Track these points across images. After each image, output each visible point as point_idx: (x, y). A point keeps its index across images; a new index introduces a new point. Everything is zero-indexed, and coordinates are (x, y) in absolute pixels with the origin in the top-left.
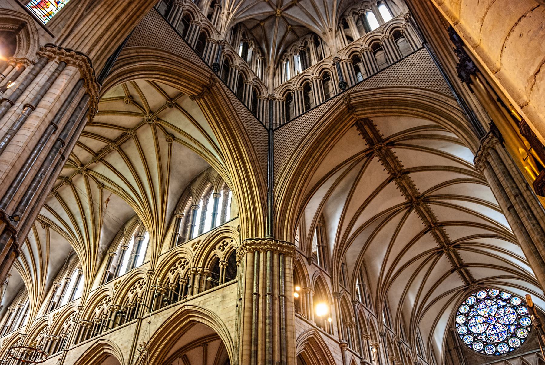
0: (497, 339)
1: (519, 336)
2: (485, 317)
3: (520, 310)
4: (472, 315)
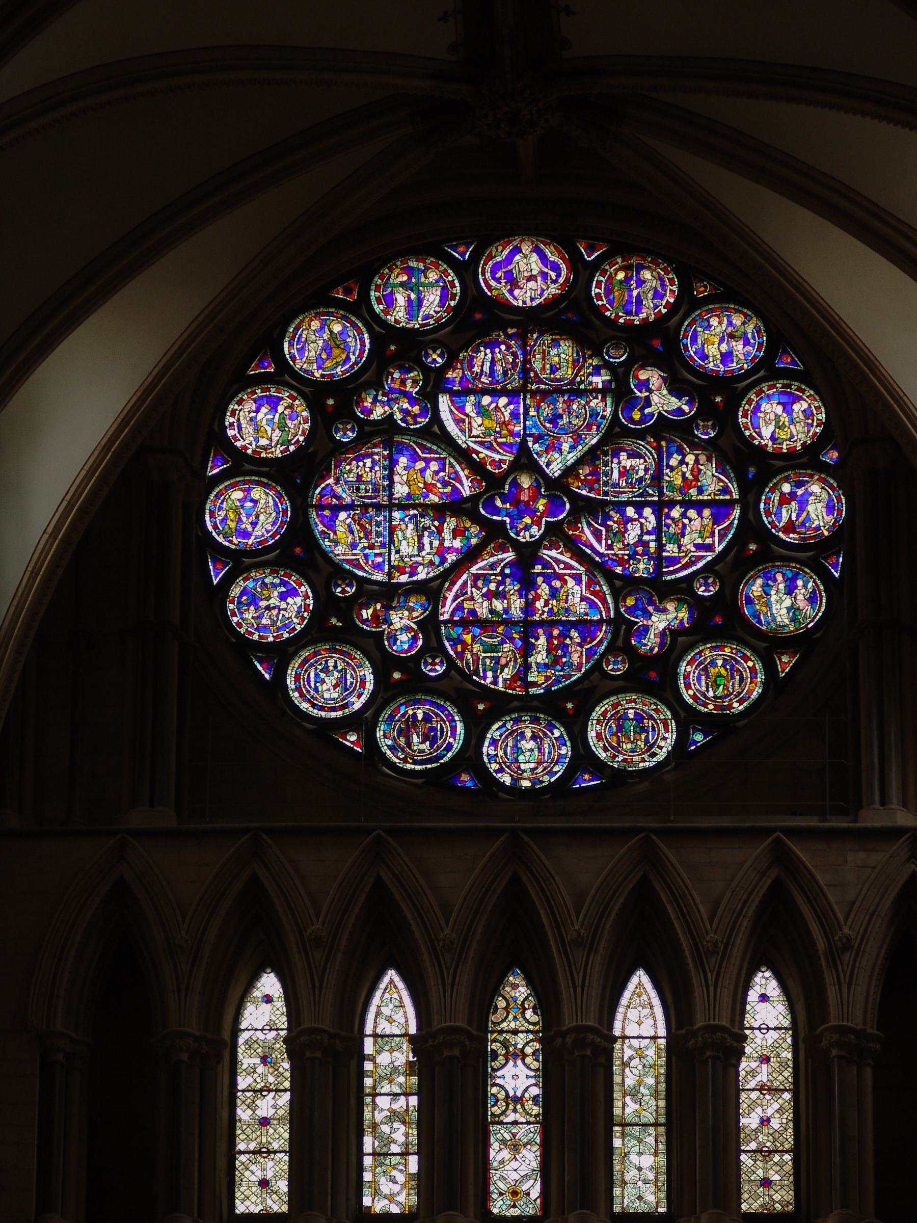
0: (507, 673)
1: (687, 696)
2: (477, 468)
3: (785, 500)
4: (378, 412)
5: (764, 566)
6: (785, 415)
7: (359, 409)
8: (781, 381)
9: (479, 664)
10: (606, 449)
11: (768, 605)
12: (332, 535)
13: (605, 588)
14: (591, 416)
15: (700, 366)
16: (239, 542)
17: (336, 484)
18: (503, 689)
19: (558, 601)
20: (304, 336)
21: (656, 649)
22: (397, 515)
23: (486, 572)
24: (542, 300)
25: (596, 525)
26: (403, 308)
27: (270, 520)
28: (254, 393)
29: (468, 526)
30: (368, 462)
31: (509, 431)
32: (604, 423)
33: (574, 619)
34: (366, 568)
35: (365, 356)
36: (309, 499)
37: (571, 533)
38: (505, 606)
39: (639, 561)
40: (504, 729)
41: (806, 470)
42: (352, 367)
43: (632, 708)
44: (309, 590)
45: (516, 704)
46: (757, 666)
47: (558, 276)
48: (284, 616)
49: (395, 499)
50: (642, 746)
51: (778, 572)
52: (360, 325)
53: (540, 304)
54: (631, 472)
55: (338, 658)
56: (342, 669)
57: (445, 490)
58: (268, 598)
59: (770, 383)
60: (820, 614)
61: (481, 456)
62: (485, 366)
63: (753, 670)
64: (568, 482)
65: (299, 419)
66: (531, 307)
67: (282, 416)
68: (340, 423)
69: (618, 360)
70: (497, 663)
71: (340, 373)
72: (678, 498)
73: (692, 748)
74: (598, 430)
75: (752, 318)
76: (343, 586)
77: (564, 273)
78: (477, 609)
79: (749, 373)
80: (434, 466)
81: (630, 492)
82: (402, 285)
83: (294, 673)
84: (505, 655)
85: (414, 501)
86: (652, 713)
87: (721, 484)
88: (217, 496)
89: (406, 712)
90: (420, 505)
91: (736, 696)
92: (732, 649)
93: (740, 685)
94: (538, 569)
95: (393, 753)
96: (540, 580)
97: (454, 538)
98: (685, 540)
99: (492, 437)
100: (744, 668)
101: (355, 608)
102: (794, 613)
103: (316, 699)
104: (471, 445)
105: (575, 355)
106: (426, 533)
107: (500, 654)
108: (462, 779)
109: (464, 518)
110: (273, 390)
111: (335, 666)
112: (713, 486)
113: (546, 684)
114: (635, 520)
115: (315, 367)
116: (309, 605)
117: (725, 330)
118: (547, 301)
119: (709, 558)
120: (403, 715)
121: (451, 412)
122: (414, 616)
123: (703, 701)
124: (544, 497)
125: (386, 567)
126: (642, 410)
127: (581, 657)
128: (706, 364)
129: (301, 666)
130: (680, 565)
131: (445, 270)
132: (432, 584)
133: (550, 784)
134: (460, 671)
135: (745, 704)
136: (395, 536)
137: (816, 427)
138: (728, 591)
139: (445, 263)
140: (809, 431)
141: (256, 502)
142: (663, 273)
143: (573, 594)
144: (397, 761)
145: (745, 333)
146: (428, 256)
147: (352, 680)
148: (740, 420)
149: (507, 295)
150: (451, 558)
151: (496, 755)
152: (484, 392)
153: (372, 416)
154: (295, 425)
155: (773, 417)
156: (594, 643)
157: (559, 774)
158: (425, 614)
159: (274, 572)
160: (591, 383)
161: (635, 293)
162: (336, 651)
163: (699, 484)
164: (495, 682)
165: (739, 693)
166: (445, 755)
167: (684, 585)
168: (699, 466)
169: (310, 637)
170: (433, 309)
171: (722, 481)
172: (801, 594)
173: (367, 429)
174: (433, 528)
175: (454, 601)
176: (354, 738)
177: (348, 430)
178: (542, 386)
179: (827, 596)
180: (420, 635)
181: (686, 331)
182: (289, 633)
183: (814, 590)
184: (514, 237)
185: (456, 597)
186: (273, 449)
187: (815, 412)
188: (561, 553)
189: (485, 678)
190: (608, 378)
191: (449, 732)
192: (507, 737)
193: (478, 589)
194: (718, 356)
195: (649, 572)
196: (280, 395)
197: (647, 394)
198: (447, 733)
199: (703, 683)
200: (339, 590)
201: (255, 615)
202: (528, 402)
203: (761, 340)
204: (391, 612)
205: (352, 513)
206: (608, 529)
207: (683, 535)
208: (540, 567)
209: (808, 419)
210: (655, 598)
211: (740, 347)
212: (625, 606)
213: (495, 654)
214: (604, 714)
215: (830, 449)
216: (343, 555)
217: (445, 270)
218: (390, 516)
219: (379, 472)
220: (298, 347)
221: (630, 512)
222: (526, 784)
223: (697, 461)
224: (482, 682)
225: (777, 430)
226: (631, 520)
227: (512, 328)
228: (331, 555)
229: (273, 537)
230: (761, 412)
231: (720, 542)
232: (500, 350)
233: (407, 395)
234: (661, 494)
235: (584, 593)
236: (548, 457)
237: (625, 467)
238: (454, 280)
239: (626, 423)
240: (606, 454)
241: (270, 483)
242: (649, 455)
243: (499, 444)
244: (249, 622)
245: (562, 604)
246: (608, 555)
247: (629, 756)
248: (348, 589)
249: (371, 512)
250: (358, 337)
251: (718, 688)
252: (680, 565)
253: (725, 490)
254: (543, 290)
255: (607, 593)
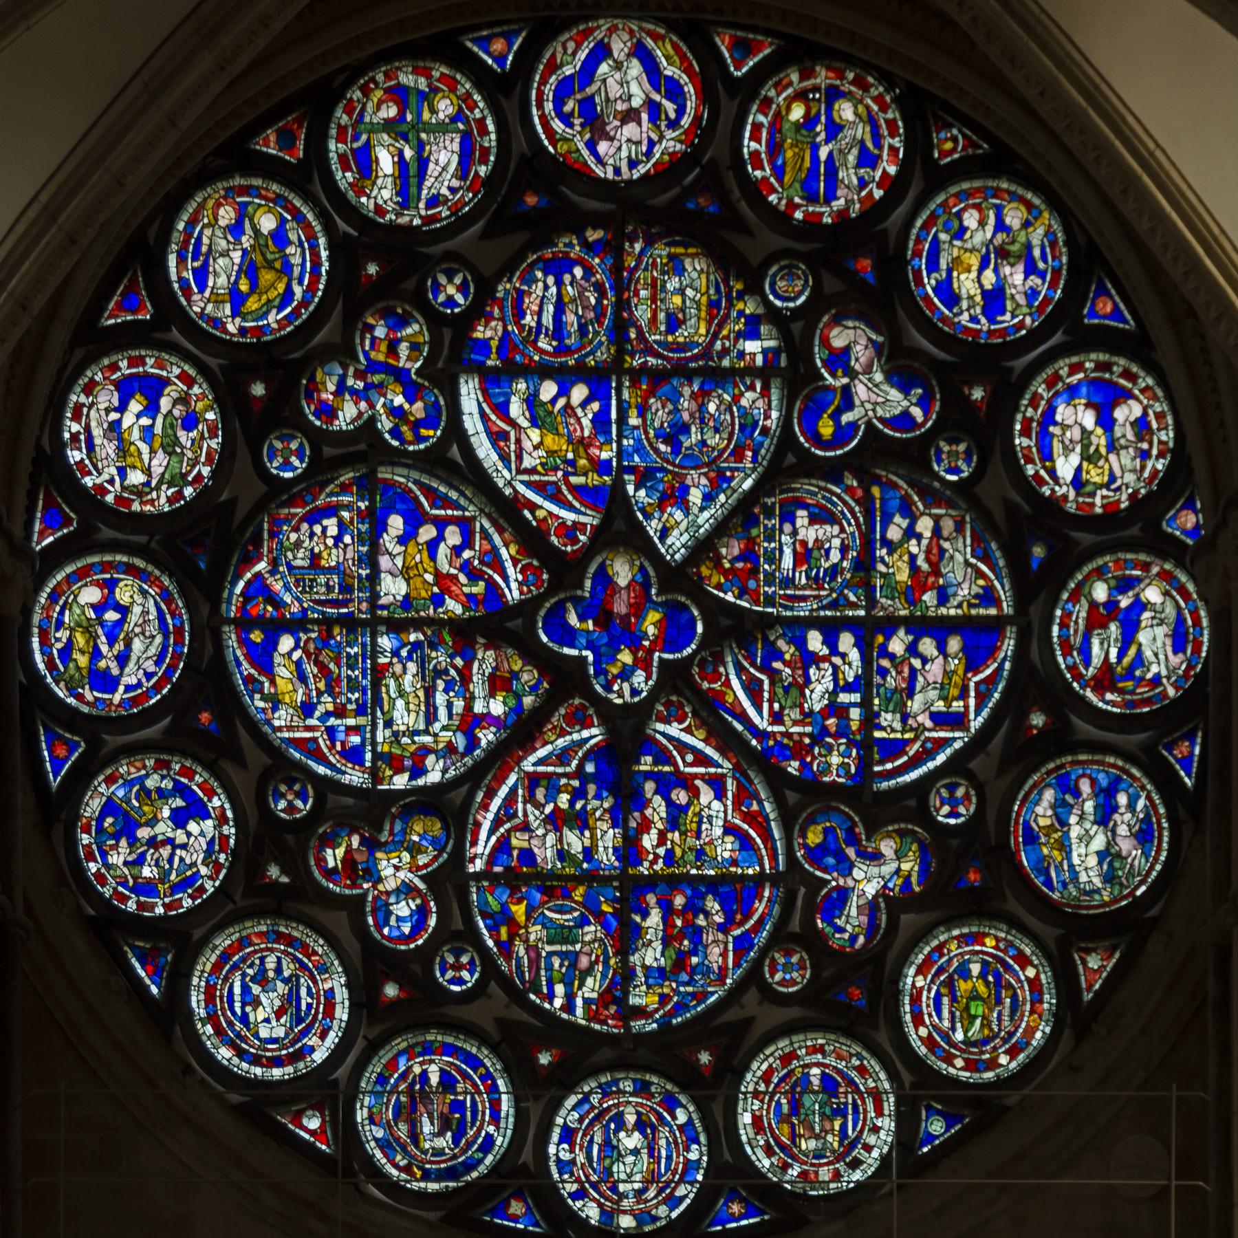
0: (591, 988)
1: (916, 1037)
3: (1099, 617)
4: (348, 412)
5: (1058, 762)
6: (1099, 431)
7: (313, 407)
8: (1093, 356)
9: (539, 969)
10: (769, 501)
11: (1064, 847)
12: (267, 685)
13: (768, 807)
14: (742, 428)
15: (944, 319)
16: (97, 699)
17: (273, 572)
18: (583, 1022)
19: (683, 834)
20: (205, 240)
21: (861, 940)
22: (385, 642)
23: (550, 769)
24: (649, 165)
25: (752, 670)
26: (390, 180)
27: (153, 651)
28: (114, 367)
29: (516, 668)
30: (332, 525)
31: (590, 459)
32: (766, 444)
33: (712, 872)
34: (331, 758)
35: (321, 287)
36: (224, 606)
37: (705, 685)
38: (587, 843)
39: (830, 749)
40: (586, 1107)
41: (1136, 552)
42: (296, 313)
43: (818, 1065)
44: (227, 806)
45: (606, 1054)
46: (1043, 977)
47: (681, 111)
48: (182, 860)
49: (383, 607)
50: (836, 1145)
51: (1084, 775)
52: (310, 217)
53: (645, 177)
54: (816, 554)
55: (283, 952)
56: (291, 976)
57: (475, 590)
58: (152, 822)
59: (1075, 359)
60: (1158, 867)
61: (541, 514)
62: (545, 314)
63: (1034, 984)
64: (699, 574)
65: (200, 427)
66: (630, 182)
67: (168, 421)
68: (277, 438)
69: (791, 305)
70: (574, 965)
71: (275, 326)
72: (903, 613)
73: (925, 1150)
74: (754, 460)
75: (1041, 213)
76: (290, 797)
77: (690, 105)
78: (536, 850)
79: (1036, 337)
80: (453, 536)
81: (815, 597)
82: (388, 125)
83: (203, 984)
84: (586, 949)
85: (417, 612)
86: (853, 1074)
87: (981, 582)
88: (54, 597)
89: (409, 1070)
90: (430, 621)
91: (1005, 1041)
92: (997, 939)
93: (1012, 1019)
94: (646, 763)
95: (386, 1155)
96: (650, 787)
97: (492, 694)
98: (915, 705)
99: (560, 474)
100: (1019, 981)
101: (312, 844)
102: (1110, 864)
103: (244, 1039)
104: (522, 489)
105: (712, 291)
106: (441, 685)
107: (578, 947)
108: (512, 1211)
109: (510, 651)
110: (150, 361)
111: (279, 970)
112: (965, 586)
113: (661, 1012)
114: (825, 659)
115: (228, 311)
116: (228, 837)
117: (991, 241)
118: (660, 168)
119: (958, 745)
120: (404, 1076)
121: (483, 415)
122: (421, 863)
123: (944, 1050)
124: (656, 606)
125: (368, 756)
126: (836, 416)
127: (724, 955)
128: (956, 315)
129: (217, 967)
130: (905, 758)
131: (468, 95)
132: (453, 794)
133: (671, 1223)
134: (506, 982)
135: (1021, 1057)
136: (384, 689)
137: (1157, 458)
138: (991, 817)
139: (469, 79)
140: (1143, 468)
141: (124, 610)
142: (875, 108)
143: (710, 817)
144: (395, 1172)
145: (1029, 247)
146: (434, 60)
147: (309, 1000)
148: (1017, 441)
149: (585, 153)
150: (487, 736)
151: (573, 1162)
152: (544, 372)
153: (337, 423)
154: (193, 441)
155: (1077, 436)
156: (747, 926)
157: (688, 1201)
158: (441, 860)
159: (161, 765)
160: (742, 354)
161: (823, 153)
162: (280, 937)
163: (941, 581)
164: (569, 1007)
165: (1011, 1034)
166: (480, 1161)
167: (912, 803)
168: (942, 542)
169: (231, 906)
170: (446, 183)
171: (982, 575)
172: (1124, 822)
173: (328, 451)
174: (453, 672)
175: (492, 832)
176: (314, 1123)
177: (292, 453)
178: (652, 361)
179: (1171, 829)
180: (432, 904)
181: (918, 241)
182: (192, 897)
183: (1148, 815)
184: (596, 18)
185: (497, 823)
186: (154, 495)
187: (1154, 425)
188: (687, 730)
189: (551, 996)
190: (772, 344)
191: (488, 1111)
192: (591, 1124)
193: (539, 806)
194: (978, 299)
195: (848, 771)
196: (164, 373)
197: (845, 380)
198: (484, 1113)
199: (946, 1013)
200: (282, 804)
201: (130, 859)
202: (626, 395)
203: (1056, 263)
204: (379, 855)
205: (303, 637)
206: (773, 675)
207: (911, 693)
208: (649, 759)
209: (1141, 440)
210: (860, 829)
211: (1018, 278)
212: (806, 846)
213: (570, 948)
214: (766, 1077)
215: (1182, 508)
216: (290, 728)
217: (468, 95)
218: (374, 644)
219: (352, 549)
220: (196, 264)
221: (815, 641)
222: (626, 1222)
223: (937, 532)
224: (547, 1006)
225: (1085, 464)
226: (814, 659)
227: (595, 228)
228: (267, 729)
229: (157, 688)
230: (1055, 423)
231: (977, 713)
232: (573, 276)
233: (401, 376)
234: (872, 603)
235: (729, 817)
236: (663, 519)
237: (804, 543)
238: (484, 119)
239: (807, 445)
240: (769, 514)
241: (150, 568)
242: (849, 516)
243: (575, 489)
244: (119, 872)
245: (691, 841)
246: (774, 733)
247: (813, 1165)
248: (299, 803)
249: (338, 634)
250: (306, 245)
251: (972, 1023)
252: (905, 758)
253: (988, 597)
254: (652, 144)
255: (772, 816)
